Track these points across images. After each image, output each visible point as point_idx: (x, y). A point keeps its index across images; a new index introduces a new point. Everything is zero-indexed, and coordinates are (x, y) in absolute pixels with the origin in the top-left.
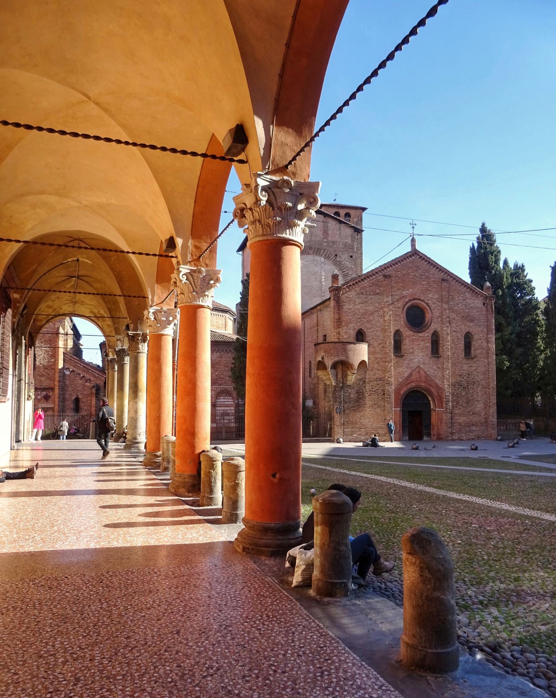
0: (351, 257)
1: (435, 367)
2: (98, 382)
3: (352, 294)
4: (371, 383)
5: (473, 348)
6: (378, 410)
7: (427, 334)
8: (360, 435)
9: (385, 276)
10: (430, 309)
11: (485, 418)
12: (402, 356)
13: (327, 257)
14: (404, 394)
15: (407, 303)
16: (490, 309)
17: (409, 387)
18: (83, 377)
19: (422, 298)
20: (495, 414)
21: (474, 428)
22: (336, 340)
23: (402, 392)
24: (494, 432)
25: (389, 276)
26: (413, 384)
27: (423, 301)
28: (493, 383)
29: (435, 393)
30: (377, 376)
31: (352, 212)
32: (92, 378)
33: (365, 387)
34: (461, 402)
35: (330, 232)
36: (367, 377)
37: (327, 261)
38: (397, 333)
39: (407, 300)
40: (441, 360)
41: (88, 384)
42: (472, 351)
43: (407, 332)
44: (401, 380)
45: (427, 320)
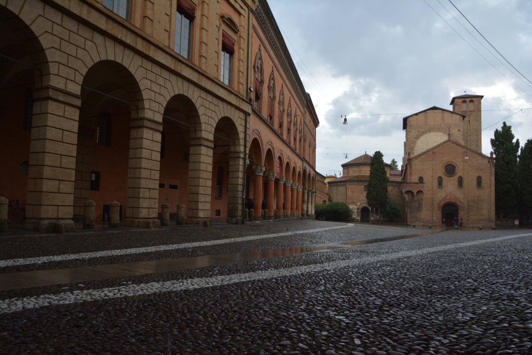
0: (459, 130)
1: (460, 193)
2: (326, 199)
3: (417, 161)
5: (482, 184)
6: (429, 212)
7: (455, 178)
8: (420, 222)
9: (433, 152)
10: (457, 166)
11: (488, 217)
12: (442, 188)
13: (445, 133)
14: (442, 205)
15: (445, 164)
16: (492, 164)
17: (445, 202)
18: (320, 197)
19: (453, 161)
20: (494, 216)
22: (409, 182)
23: (442, 204)
24: (493, 224)
25: (436, 152)
26: (447, 201)
27: (453, 162)
28: (493, 200)
29: (460, 205)
31: (474, 99)
32: (323, 197)
34: (474, 209)
36: (424, 197)
38: (440, 178)
39: (445, 162)
40: (463, 189)
41: (322, 200)
42: (482, 185)
43: (444, 177)
44: (441, 199)
45: (456, 171)
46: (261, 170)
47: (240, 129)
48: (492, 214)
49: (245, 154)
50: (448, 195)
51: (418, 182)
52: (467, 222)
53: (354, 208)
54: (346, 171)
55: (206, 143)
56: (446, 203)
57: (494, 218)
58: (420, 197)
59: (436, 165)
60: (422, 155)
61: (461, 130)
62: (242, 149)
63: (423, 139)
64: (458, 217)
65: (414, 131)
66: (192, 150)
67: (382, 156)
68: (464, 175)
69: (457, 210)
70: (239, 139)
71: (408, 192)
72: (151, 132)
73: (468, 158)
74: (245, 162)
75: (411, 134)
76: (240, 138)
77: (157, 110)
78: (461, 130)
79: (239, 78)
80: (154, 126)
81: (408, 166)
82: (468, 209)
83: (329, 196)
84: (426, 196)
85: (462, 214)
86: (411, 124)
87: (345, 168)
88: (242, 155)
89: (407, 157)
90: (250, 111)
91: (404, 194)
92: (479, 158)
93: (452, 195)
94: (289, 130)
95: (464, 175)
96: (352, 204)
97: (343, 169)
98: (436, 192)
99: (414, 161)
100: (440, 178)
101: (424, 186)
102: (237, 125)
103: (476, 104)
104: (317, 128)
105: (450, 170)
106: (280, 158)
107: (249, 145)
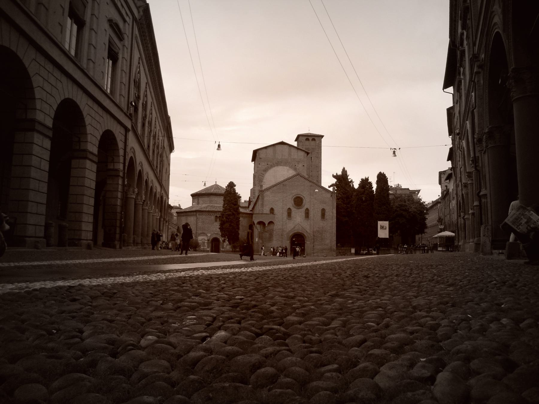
0: (304, 166)
1: (306, 224)
3: (268, 193)
4: (276, 231)
6: (279, 242)
7: (303, 210)
9: (283, 185)
14: (291, 236)
15: (294, 196)
17: (294, 232)
19: (301, 194)
21: (325, 251)
22: (261, 213)
24: (334, 253)
25: (286, 185)
26: (296, 231)
30: (279, 228)
31: (316, 138)
32: (172, 228)
33: (273, 232)
35: (292, 154)
36: (275, 228)
37: (290, 169)
38: (289, 209)
39: (294, 195)
40: (309, 221)
42: (325, 217)
43: (293, 209)
44: (290, 230)
45: (303, 204)
46: (134, 192)
47: (121, 145)
48: (333, 244)
49: (124, 173)
50: (296, 225)
51: (270, 213)
52: (312, 252)
53: (204, 239)
54: (196, 200)
55: (91, 157)
56: (294, 233)
57: (335, 248)
58: (271, 228)
59: (286, 197)
60: (273, 187)
61: (305, 165)
62: (121, 167)
63: (271, 172)
64: (304, 247)
65: (263, 164)
66: (74, 163)
67: (235, 186)
68: (310, 207)
69: (304, 241)
70: (119, 156)
71: (260, 223)
72: (41, 137)
73: (317, 191)
74: (124, 181)
75: (260, 166)
76: (120, 155)
77: (47, 112)
78: (305, 165)
79: (121, 89)
80: (46, 131)
81: (260, 197)
82: (314, 239)
83: (178, 227)
84: (277, 226)
85: (308, 244)
86: (261, 157)
87: (195, 197)
88: (121, 174)
89: (258, 188)
90: (130, 127)
91: (256, 225)
92: (323, 192)
93: (300, 226)
94: (154, 151)
95: (310, 207)
96: (202, 235)
97: (193, 199)
98: (286, 223)
99: (266, 192)
100: (289, 209)
101: (274, 218)
102: (118, 140)
103: (318, 142)
104: (171, 154)
105: (298, 202)
106: (146, 182)
107: (127, 164)
